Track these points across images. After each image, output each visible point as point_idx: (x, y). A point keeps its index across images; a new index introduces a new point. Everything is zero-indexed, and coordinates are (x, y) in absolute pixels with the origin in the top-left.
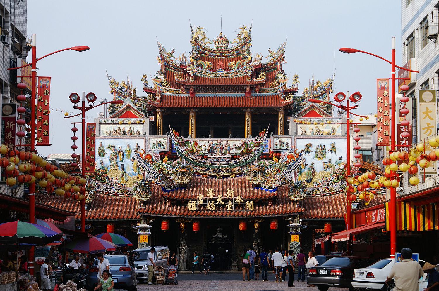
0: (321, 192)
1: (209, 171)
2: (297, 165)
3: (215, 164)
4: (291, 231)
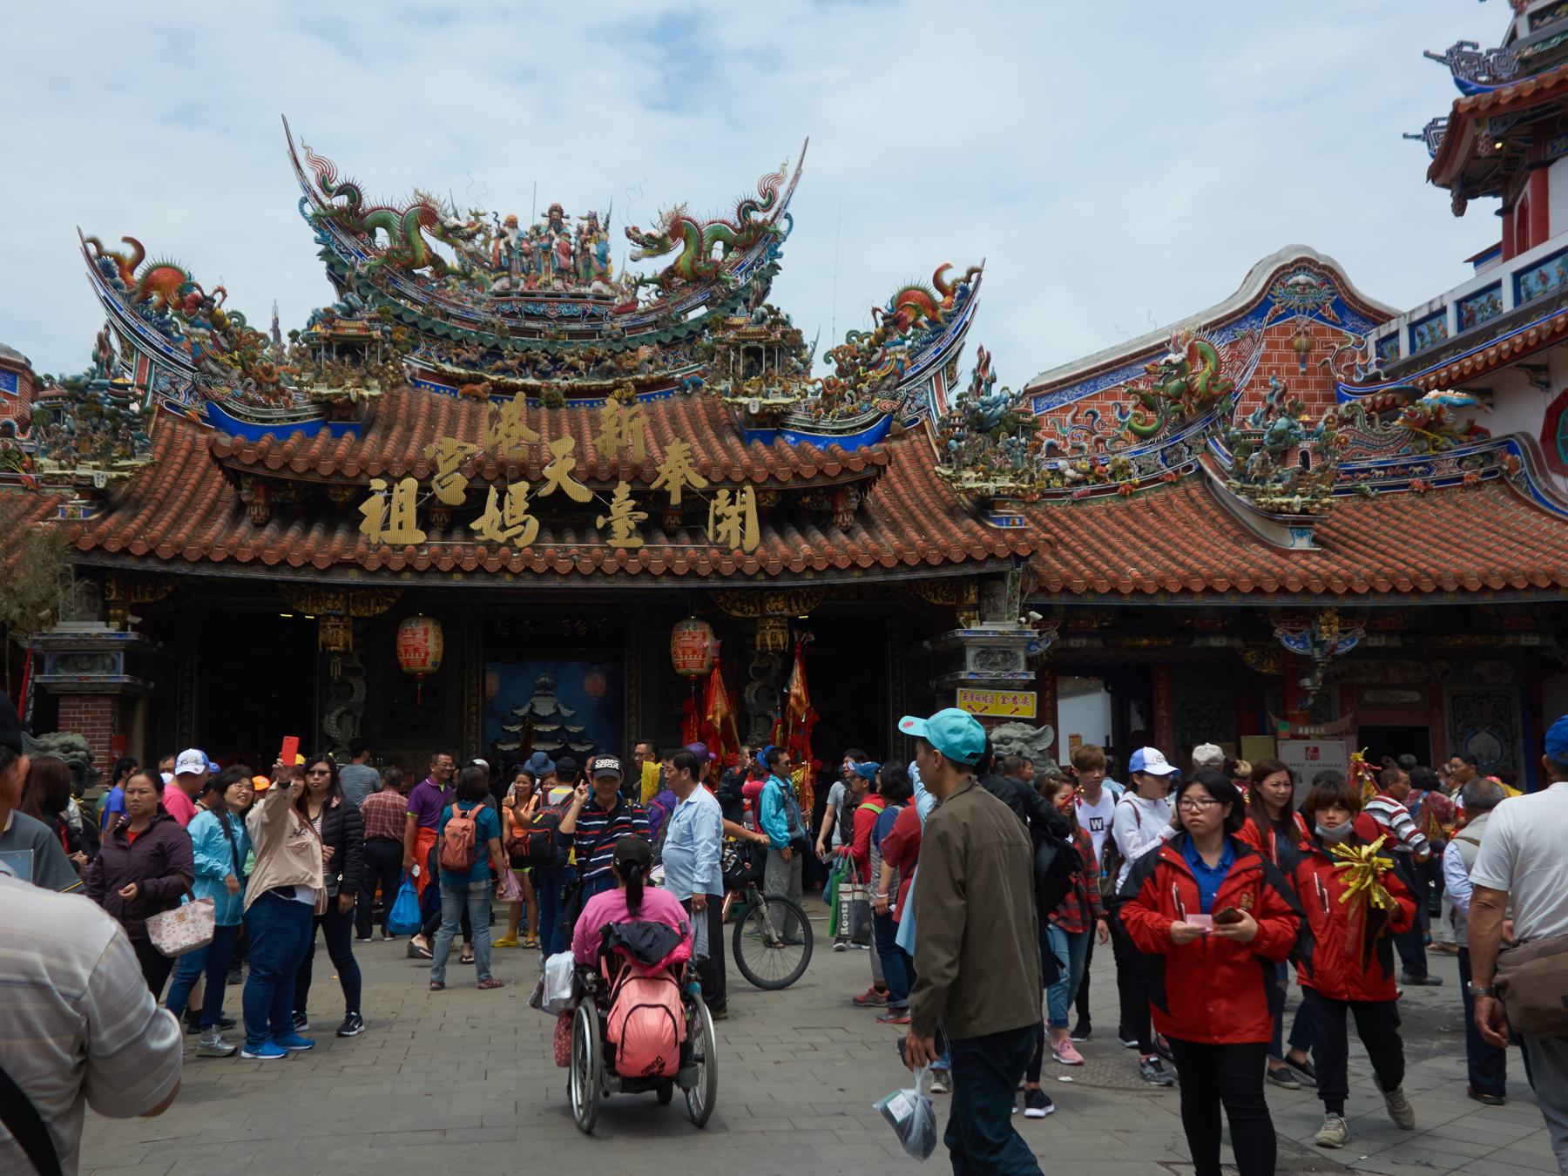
0: (1067, 480)
1: (499, 363)
2: (945, 344)
3: (531, 332)
4: (971, 667)
